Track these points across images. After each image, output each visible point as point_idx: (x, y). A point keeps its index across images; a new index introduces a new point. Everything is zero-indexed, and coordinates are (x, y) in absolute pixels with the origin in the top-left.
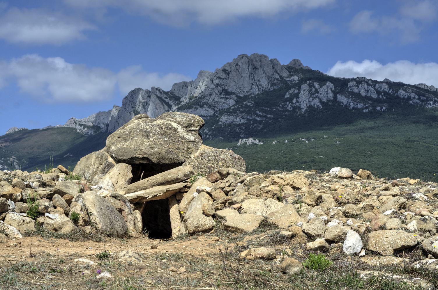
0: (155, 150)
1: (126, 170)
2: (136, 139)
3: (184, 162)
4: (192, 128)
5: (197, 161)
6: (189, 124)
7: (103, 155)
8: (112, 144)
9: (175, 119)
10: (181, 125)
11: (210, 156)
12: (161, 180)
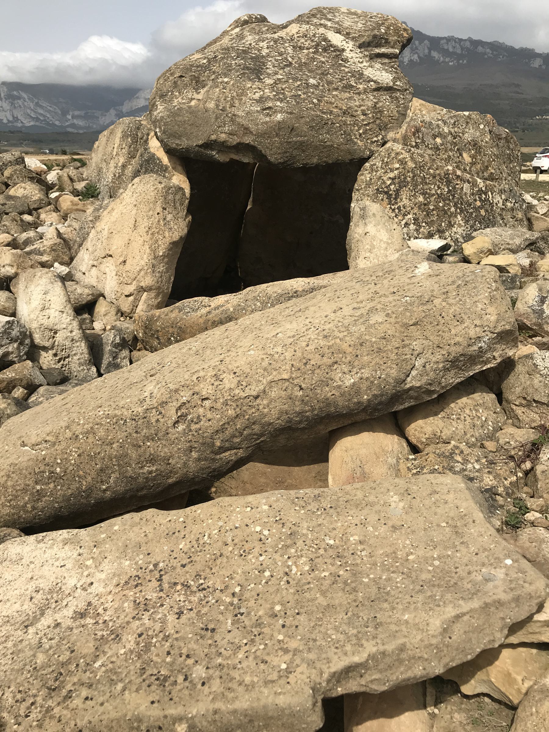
0: (279, 117)
1: (159, 209)
2: (226, 80)
3: (367, 159)
4: (383, 50)
5: (412, 158)
6: (375, 36)
7: (138, 128)
8: (162, 96)
9: (337, 23)
10: (353, 39)
11: (440, 135)
12: (279, 406)
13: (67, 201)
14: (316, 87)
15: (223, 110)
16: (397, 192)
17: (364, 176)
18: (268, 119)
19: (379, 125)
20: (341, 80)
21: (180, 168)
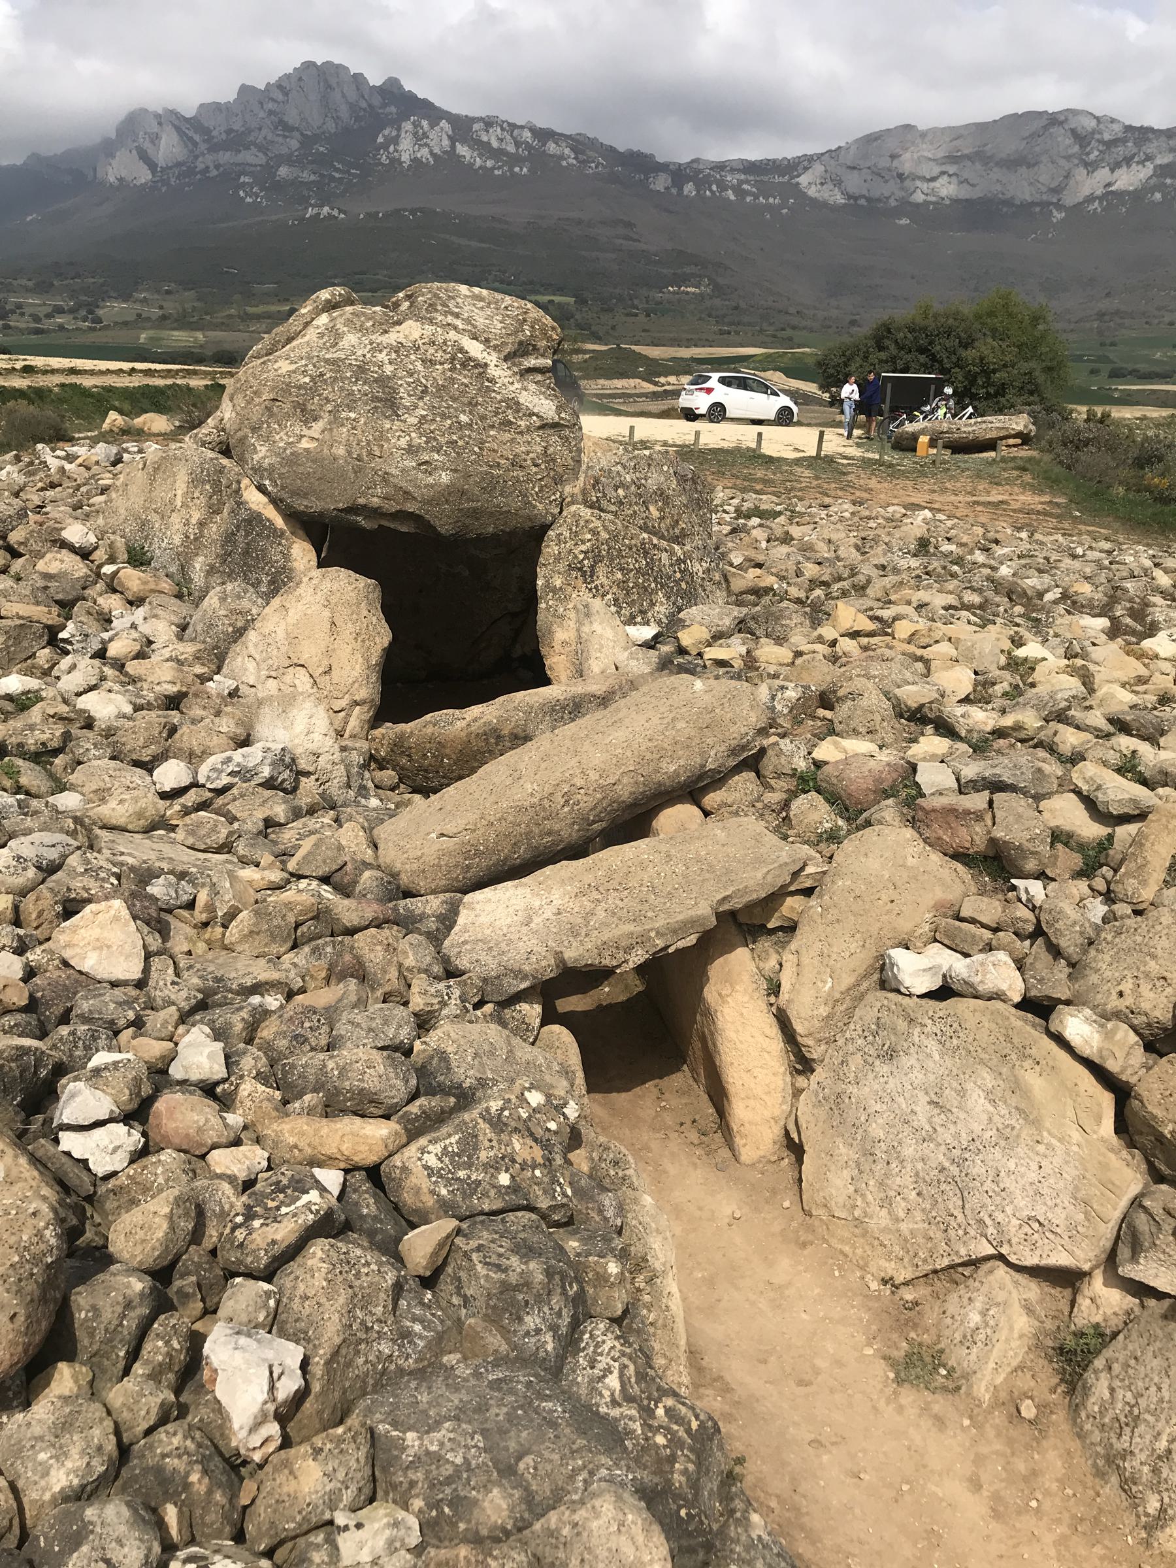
0: (445, 478)
1: (365, 613)
2: (352, 415)
6: (521, 343)
7: (221, 472)
8: (254, 430)
9: (468, 321)
10: (495, 347)
15: (359, 459)
16: (592, 568)
17: (550, 549)
18: (430, 480)
19: (554, 479)
20: (496, 414)
21: (301, 532)
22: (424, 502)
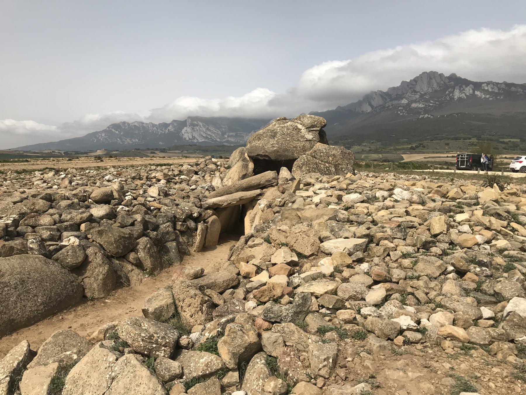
0: (275, 149)
4: (314, 129)
11: (322, 152)
13: (222, 169)
14: (289, 140)
17: (295, 163)
22: (269, 153)
